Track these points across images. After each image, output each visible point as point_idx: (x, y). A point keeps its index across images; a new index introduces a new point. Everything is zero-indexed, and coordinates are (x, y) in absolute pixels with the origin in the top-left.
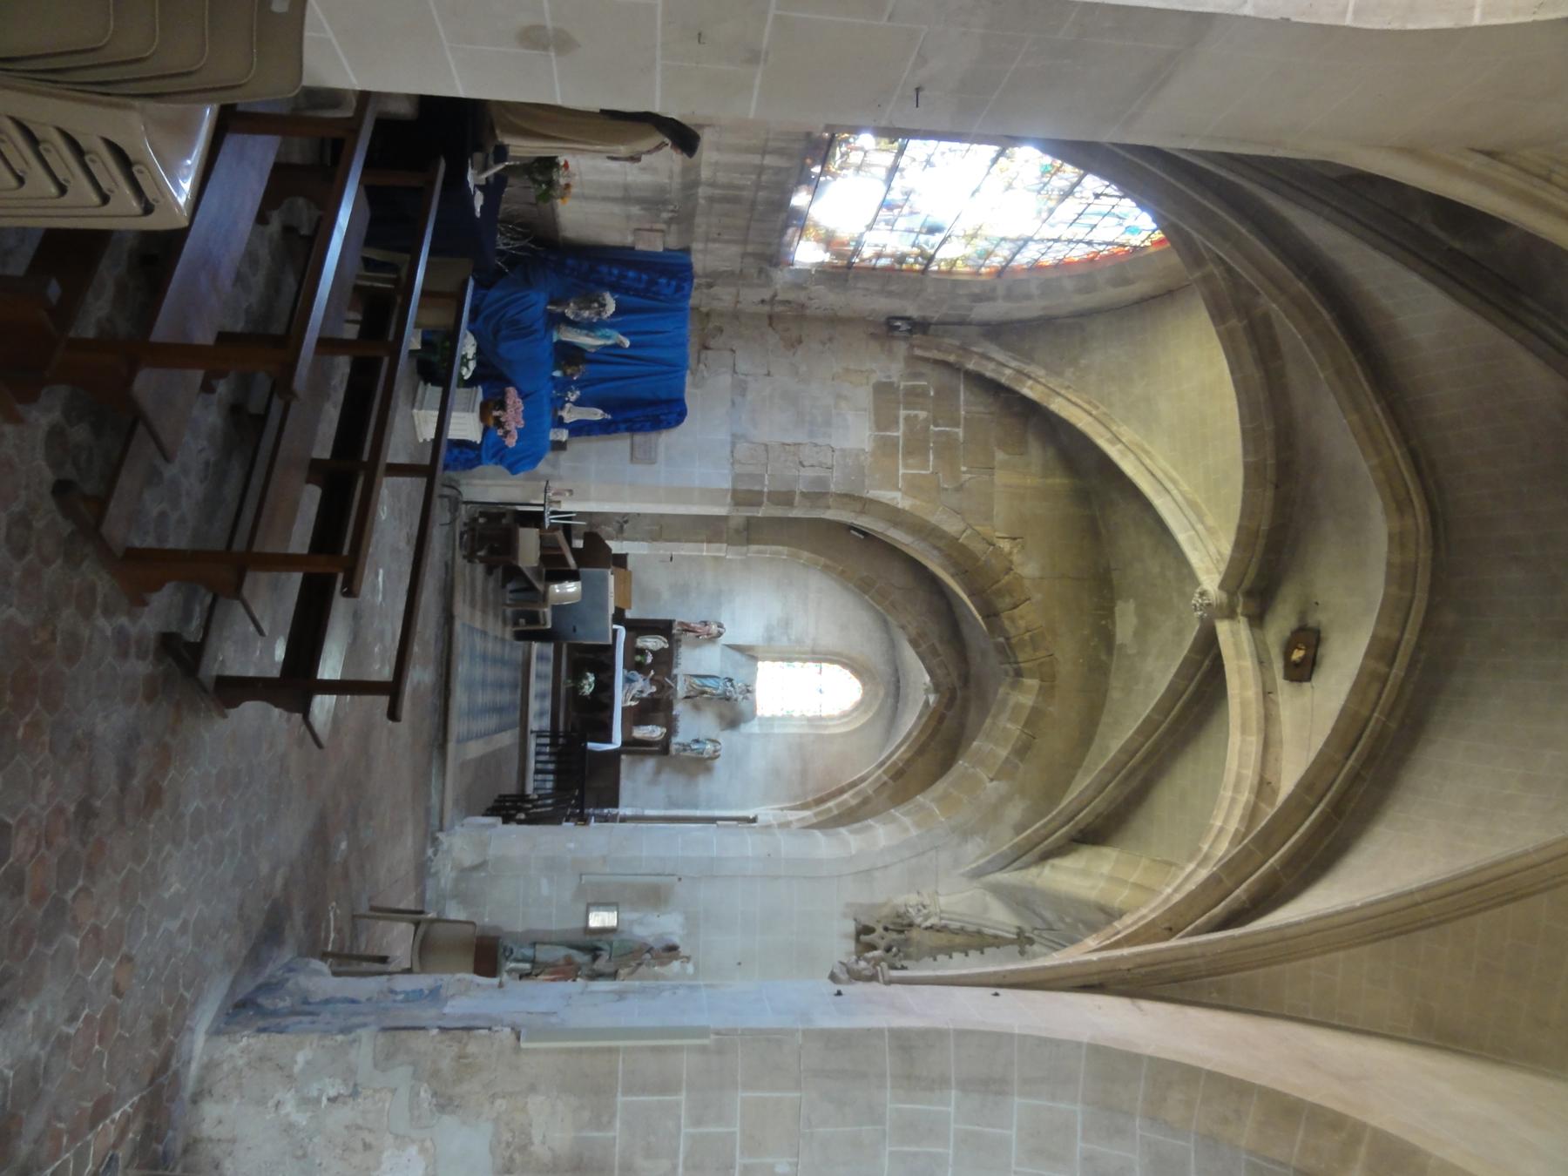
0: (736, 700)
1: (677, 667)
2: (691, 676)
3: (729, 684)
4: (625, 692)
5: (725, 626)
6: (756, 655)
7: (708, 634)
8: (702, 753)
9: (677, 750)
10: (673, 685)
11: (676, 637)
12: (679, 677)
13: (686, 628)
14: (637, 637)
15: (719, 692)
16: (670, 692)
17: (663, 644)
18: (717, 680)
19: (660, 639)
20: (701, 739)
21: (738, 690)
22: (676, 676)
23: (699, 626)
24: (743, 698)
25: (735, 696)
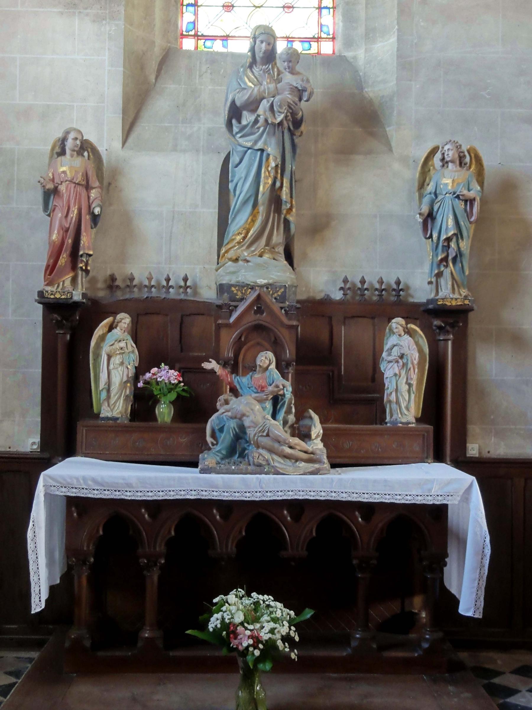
0: (299, 93)
1: (195, 288)
2: (220, 245)
3: (247, 118)
4: (278, 462)
5: (60, 135)
6: (157, 52)
7: (88, 187)
8: (472, 201)
9: (456, 284)
10: (251, 297)
11: (101, 294)
12: (225, 280)
13: (64, 259)
14: (97, 416)
15: (272, 150)
16: (276, 307)
17: (117, 332)
18: (235, 159)
19: (102, 338)
20: (425, 209)
21: (268, 85)
22: (222, 289)
23: (59, 215)
24: (292, 72)
25: (288, 96)
